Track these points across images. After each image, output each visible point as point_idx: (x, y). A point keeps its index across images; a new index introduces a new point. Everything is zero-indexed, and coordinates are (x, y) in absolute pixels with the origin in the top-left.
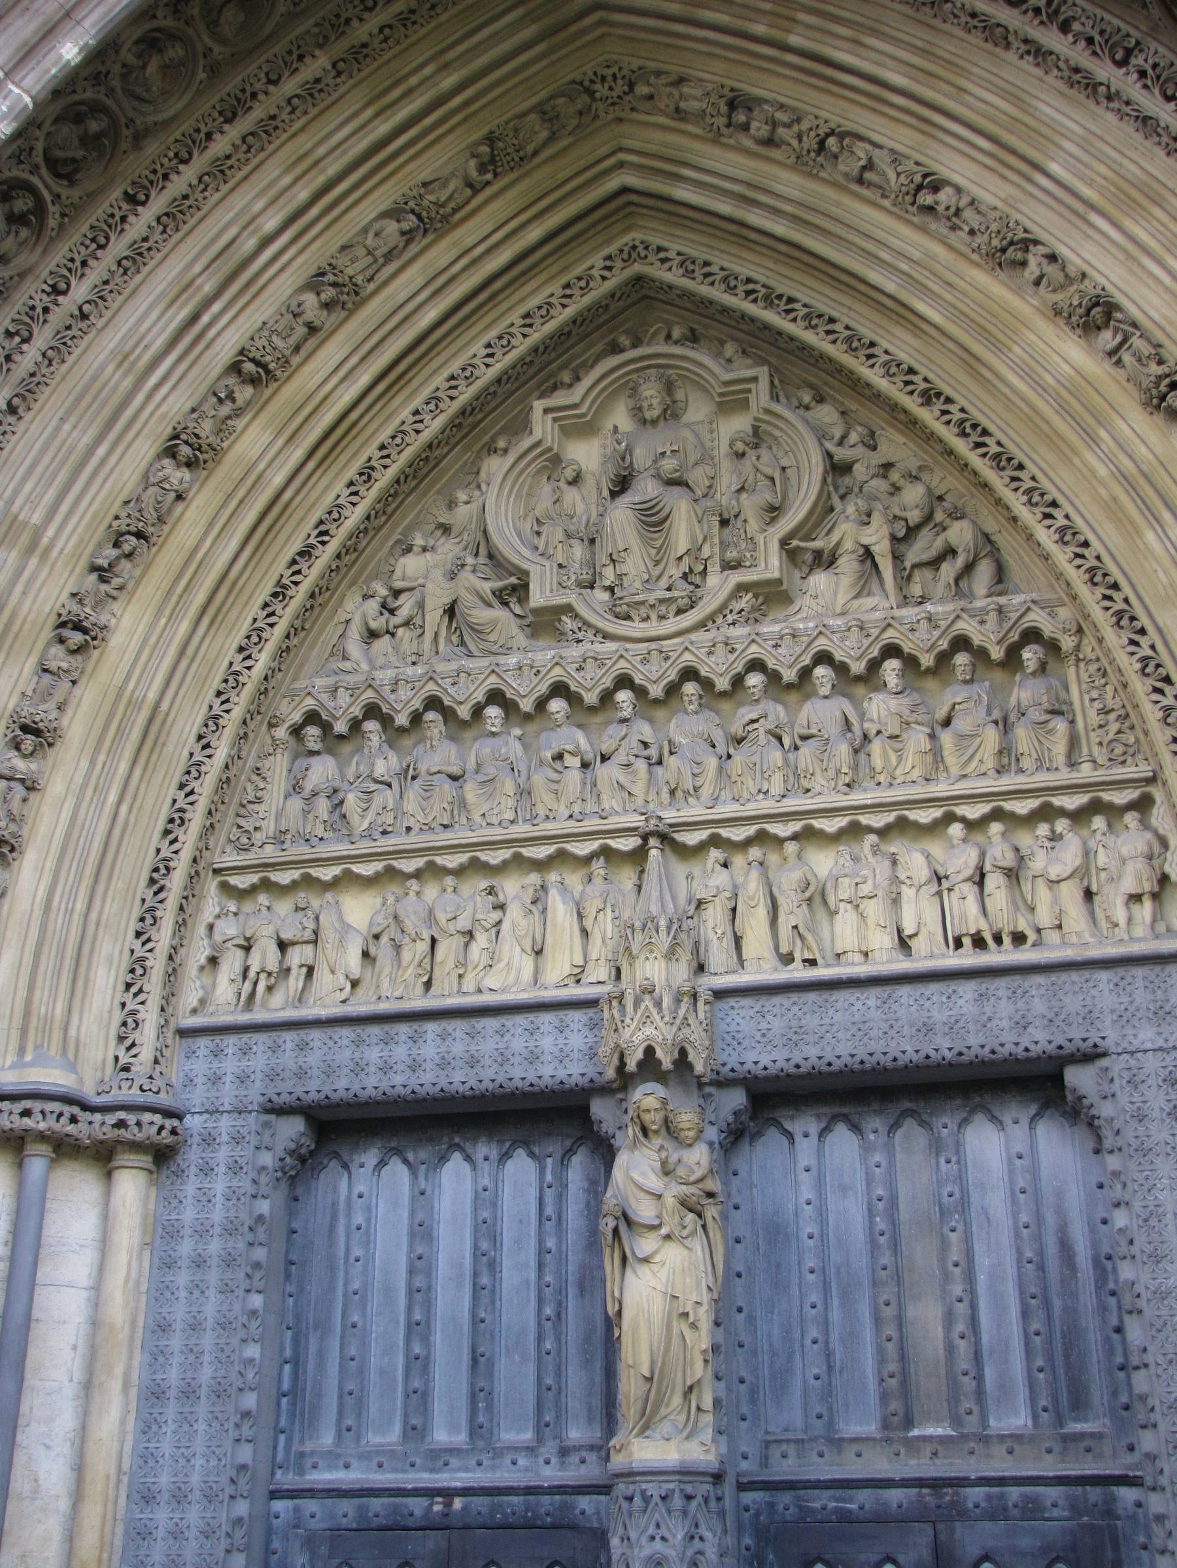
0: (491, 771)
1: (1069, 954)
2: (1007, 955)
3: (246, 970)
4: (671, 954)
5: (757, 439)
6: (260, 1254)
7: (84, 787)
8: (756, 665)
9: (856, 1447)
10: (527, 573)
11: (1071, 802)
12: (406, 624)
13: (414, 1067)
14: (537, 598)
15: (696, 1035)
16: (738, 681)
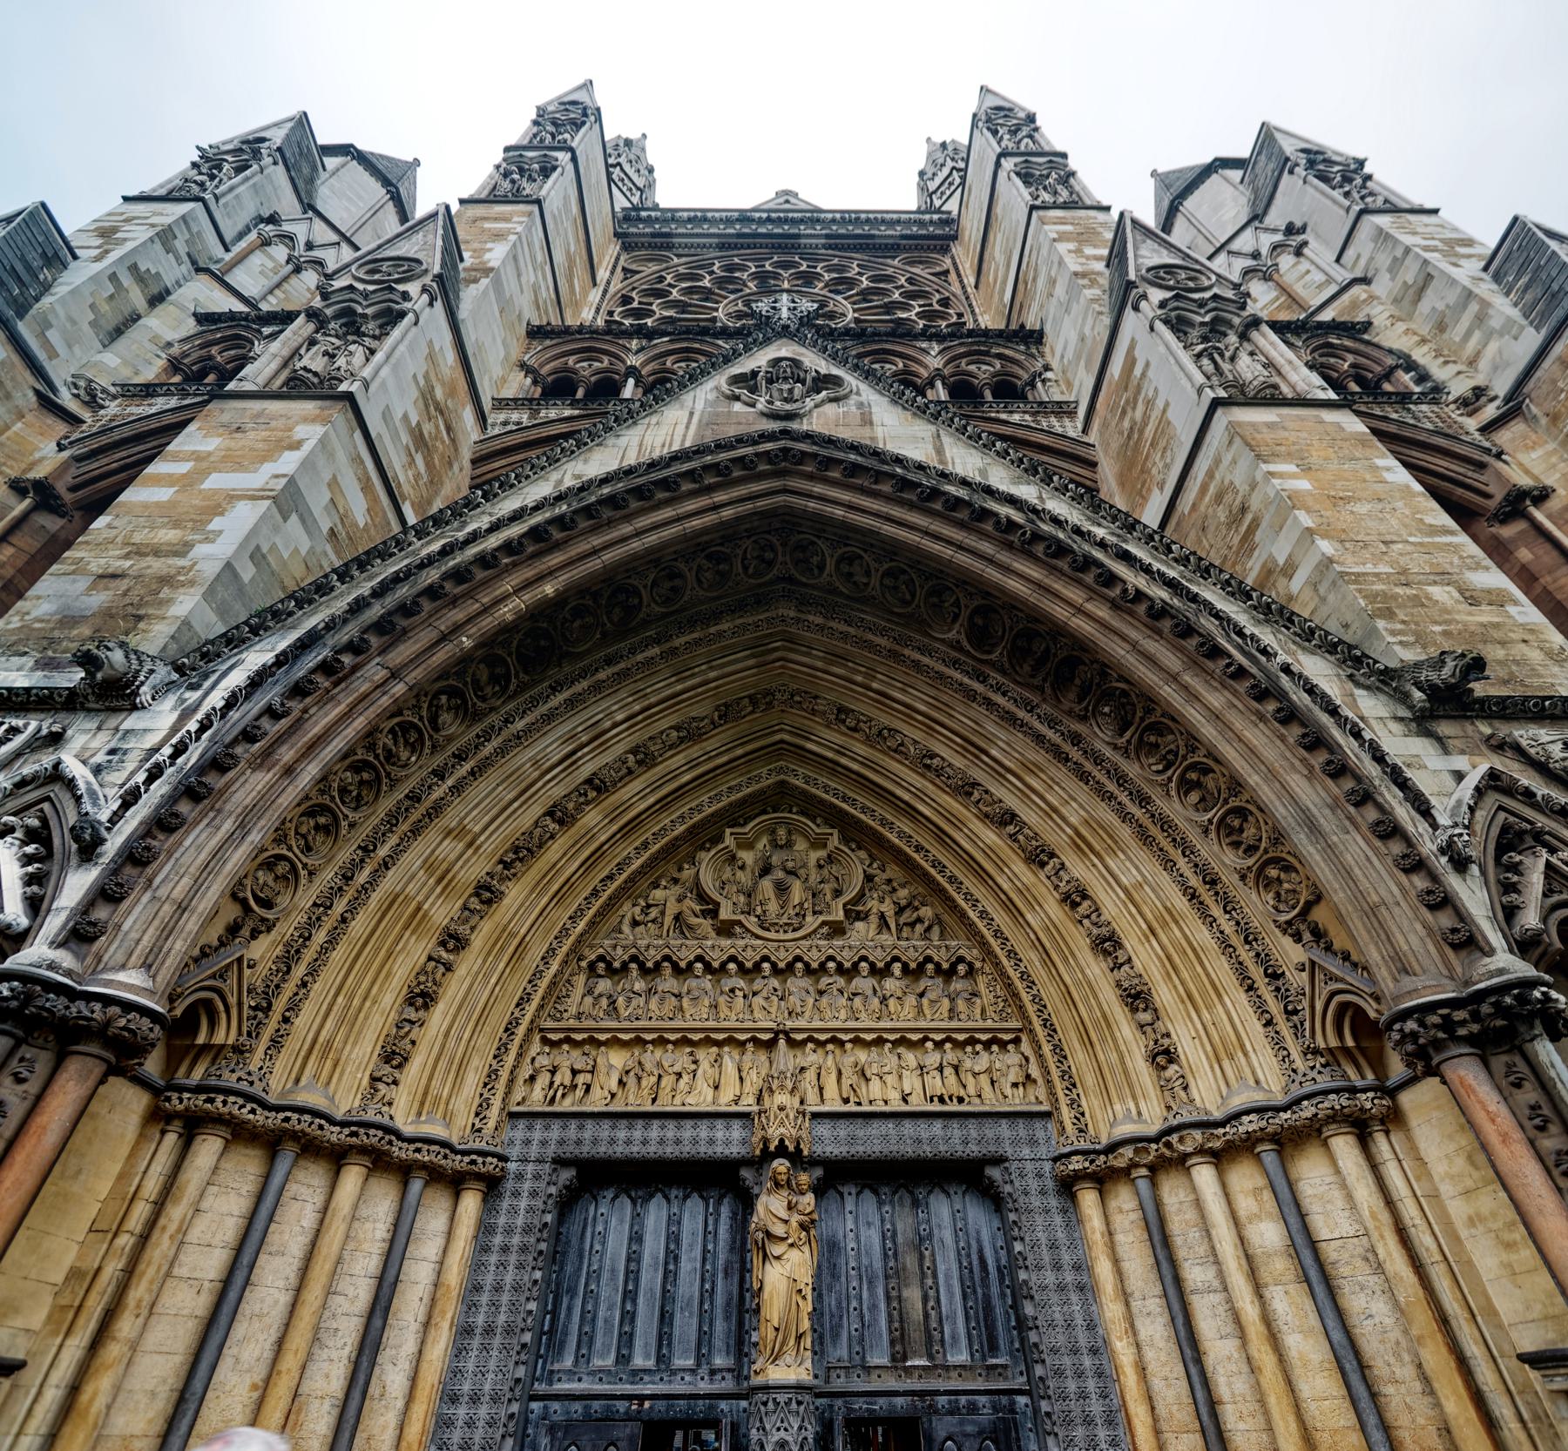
0: (696, 994)
1: (987, 1108)
2: (953, 1107)
3: (552, 1083)
4: (792, 1092)
5: (830, 859)
6: (543, 1246)
7: (478, 973)
8: (831, 958)
9: (878, 1372)
10: (718, 904)
11: (984, 1037)
12: (653, 921)
13: (645, 1142)
14: (725, 914)
15: (804, 1134)
16: (822, 965)
